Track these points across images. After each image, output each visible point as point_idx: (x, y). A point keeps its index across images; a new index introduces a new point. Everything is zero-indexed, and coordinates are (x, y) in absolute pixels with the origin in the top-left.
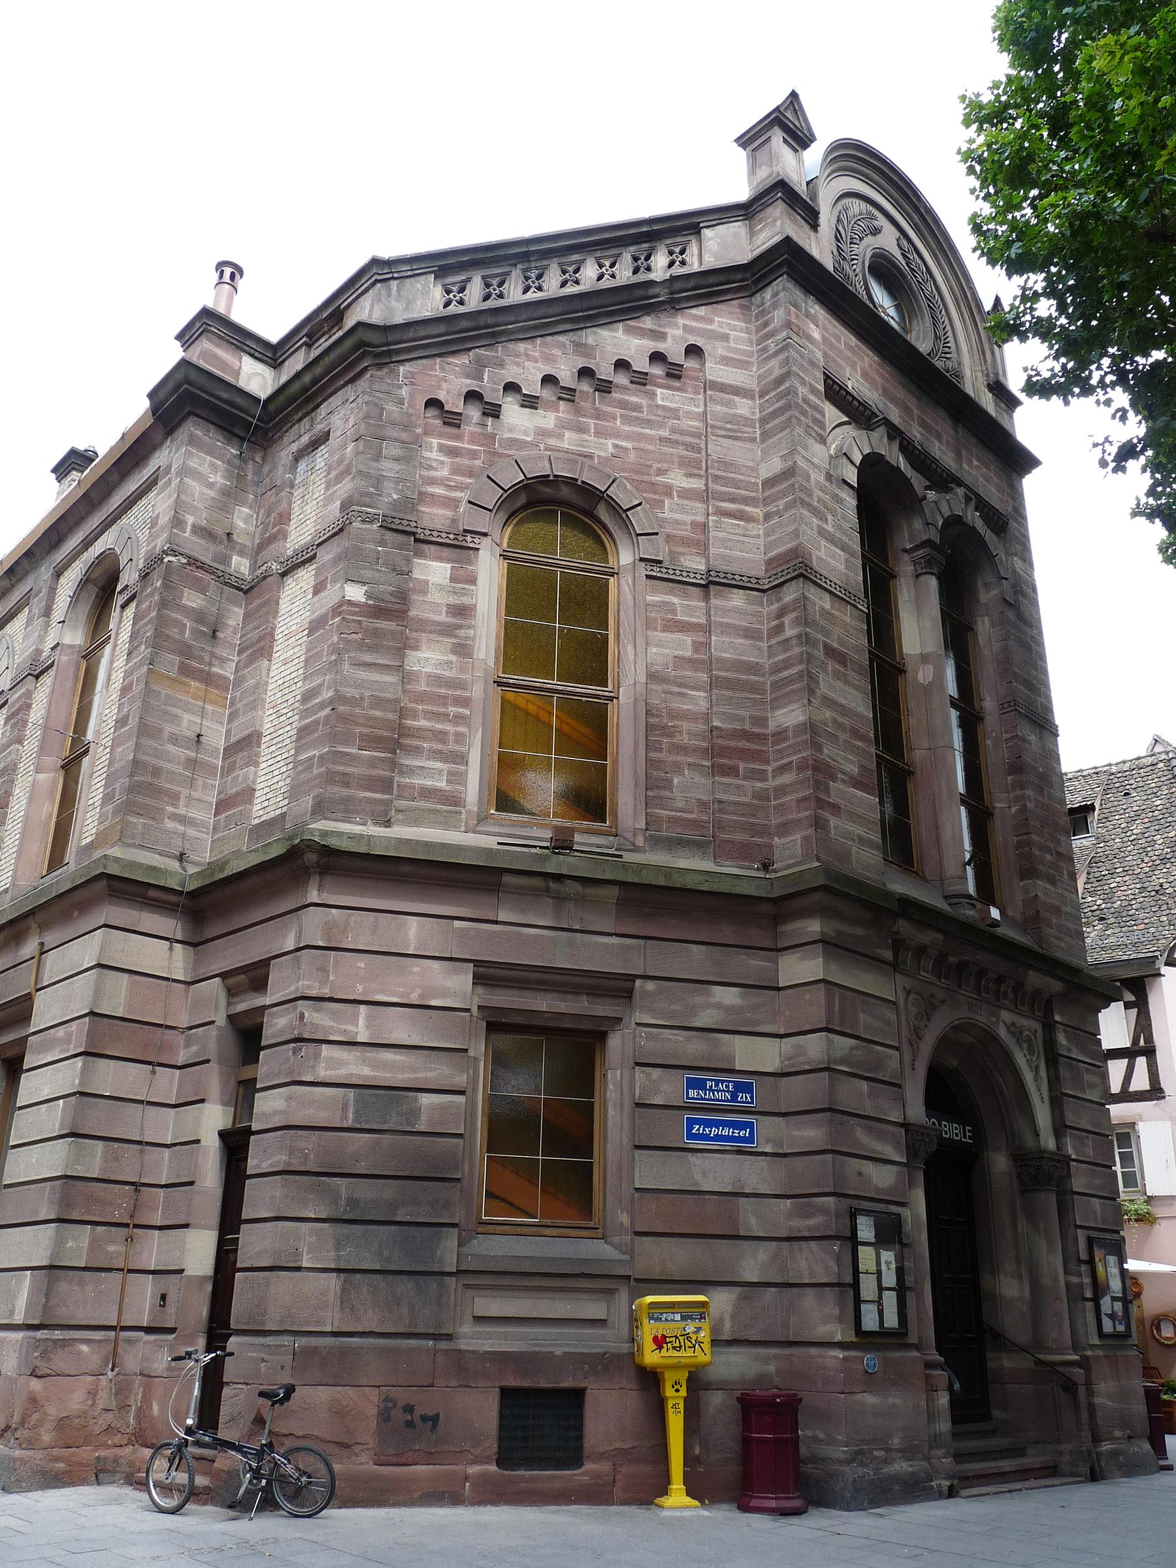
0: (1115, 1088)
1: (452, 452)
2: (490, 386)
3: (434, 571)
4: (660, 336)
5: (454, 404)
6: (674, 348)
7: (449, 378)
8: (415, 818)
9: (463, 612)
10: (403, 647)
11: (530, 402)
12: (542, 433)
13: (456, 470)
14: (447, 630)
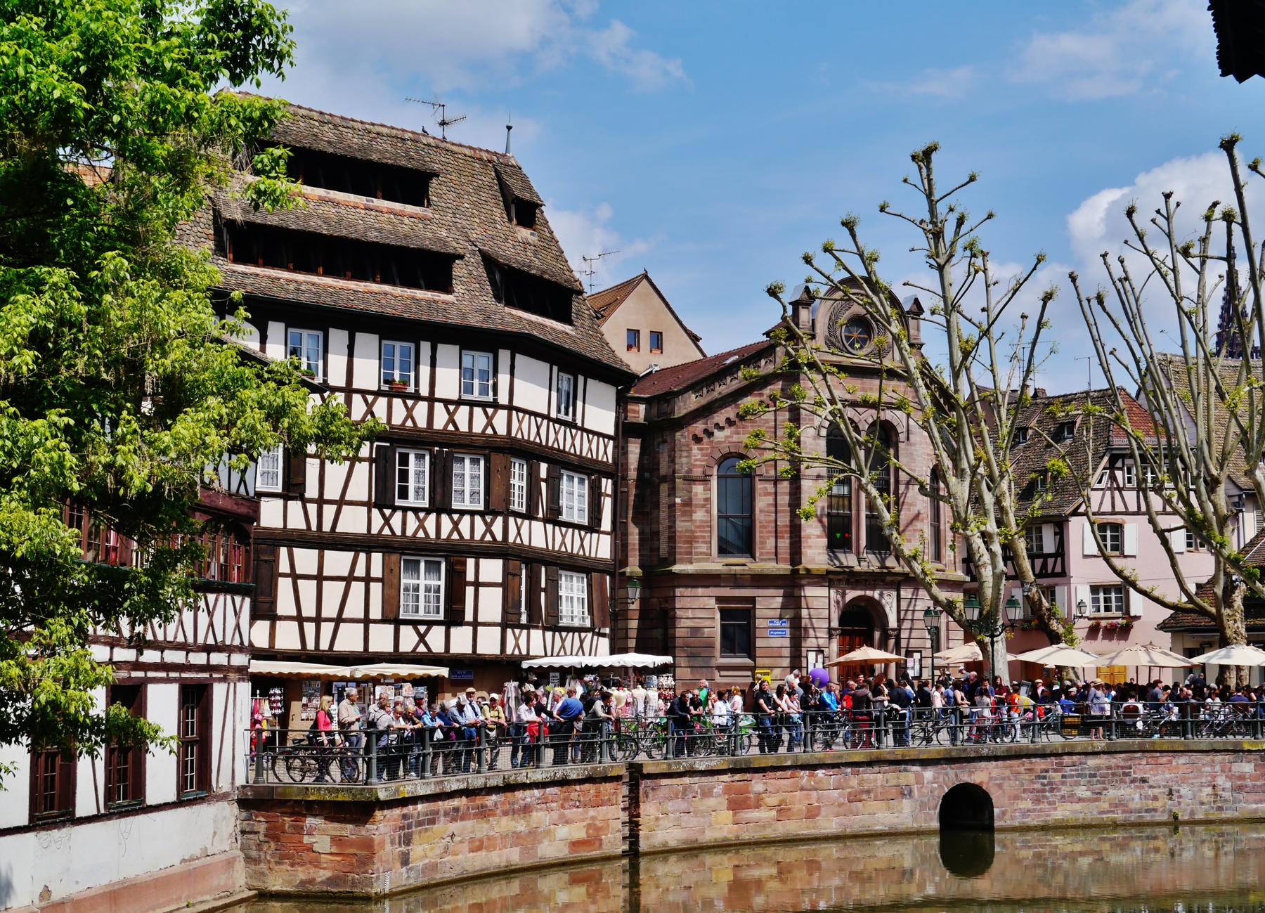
0: (1050, 571)
1: (701, 449)
2: (710, 426)
3: (698, 489)
4: (761, 395)
5: (701, 435)
6: (765, 398)
7: (698, 427)
8: (698, 560)
9: (708, 500)
10: (690, 514)
11: (722, 428)
12: (727, 437)
13: (703, 455)
14: (703, 506)
